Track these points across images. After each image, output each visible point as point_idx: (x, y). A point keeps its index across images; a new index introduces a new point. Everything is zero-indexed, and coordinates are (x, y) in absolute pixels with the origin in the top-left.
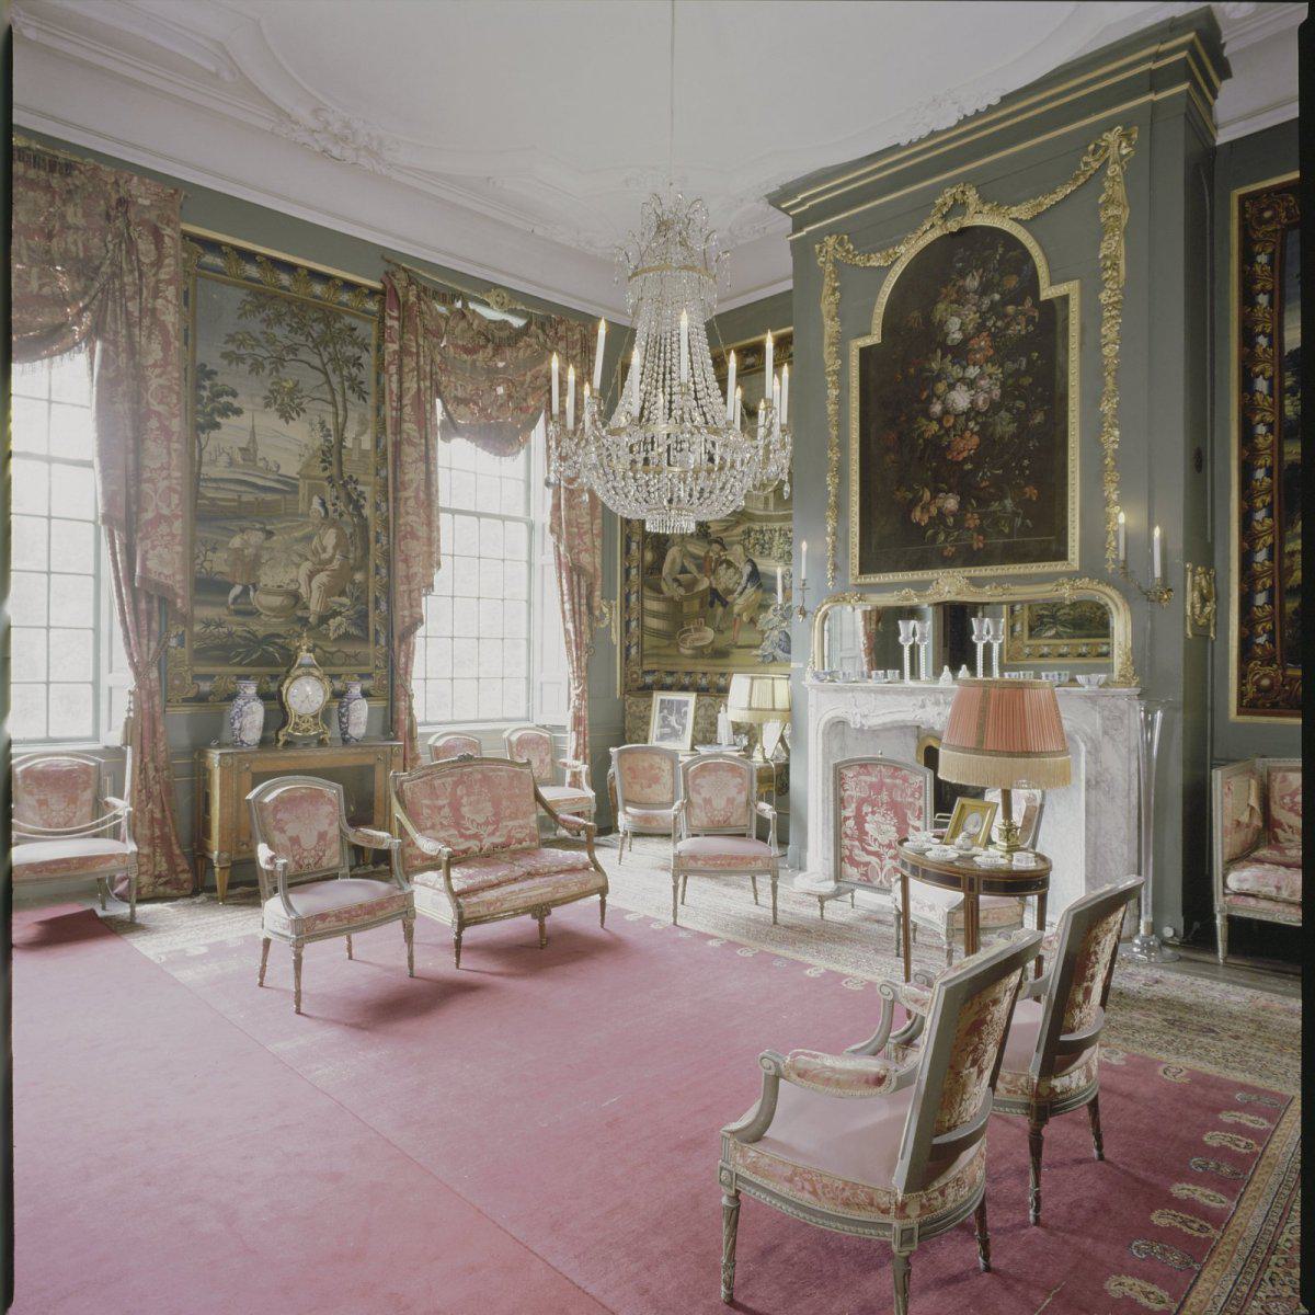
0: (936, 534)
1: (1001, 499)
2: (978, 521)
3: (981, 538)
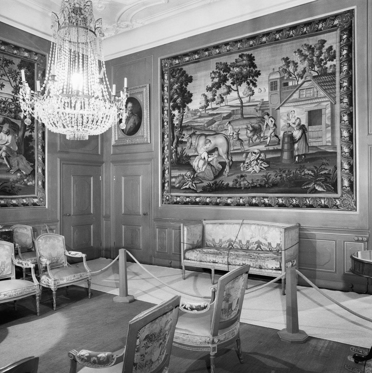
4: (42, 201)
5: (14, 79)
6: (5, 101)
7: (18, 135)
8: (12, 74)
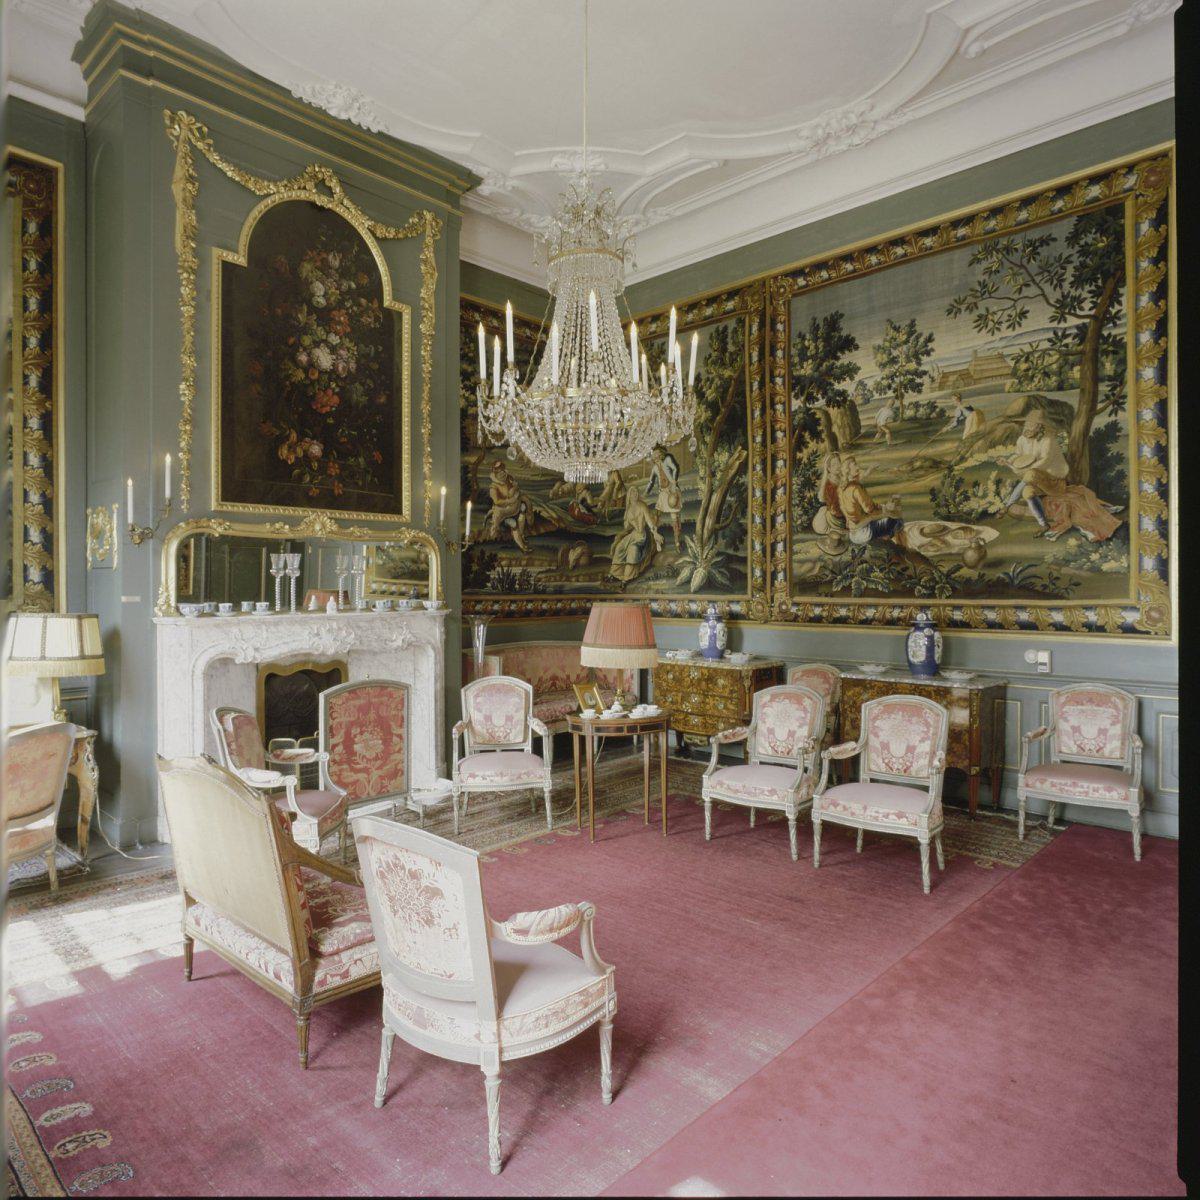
0: (300, 477)
1: (356, 456)
2: (338, 471)
3: (341, 485)
4: (1156, 621)
5: (1055, 282)
6: (1029, 354)
7: (1069, 433)
8: (1049, 271)
